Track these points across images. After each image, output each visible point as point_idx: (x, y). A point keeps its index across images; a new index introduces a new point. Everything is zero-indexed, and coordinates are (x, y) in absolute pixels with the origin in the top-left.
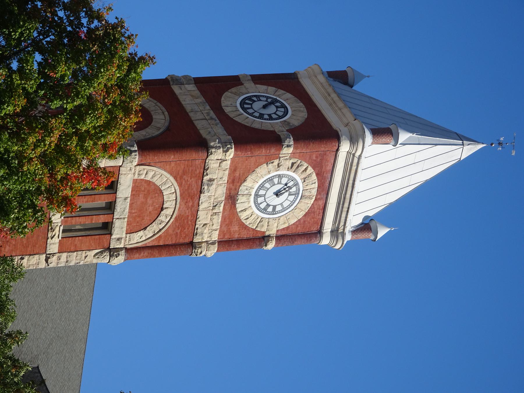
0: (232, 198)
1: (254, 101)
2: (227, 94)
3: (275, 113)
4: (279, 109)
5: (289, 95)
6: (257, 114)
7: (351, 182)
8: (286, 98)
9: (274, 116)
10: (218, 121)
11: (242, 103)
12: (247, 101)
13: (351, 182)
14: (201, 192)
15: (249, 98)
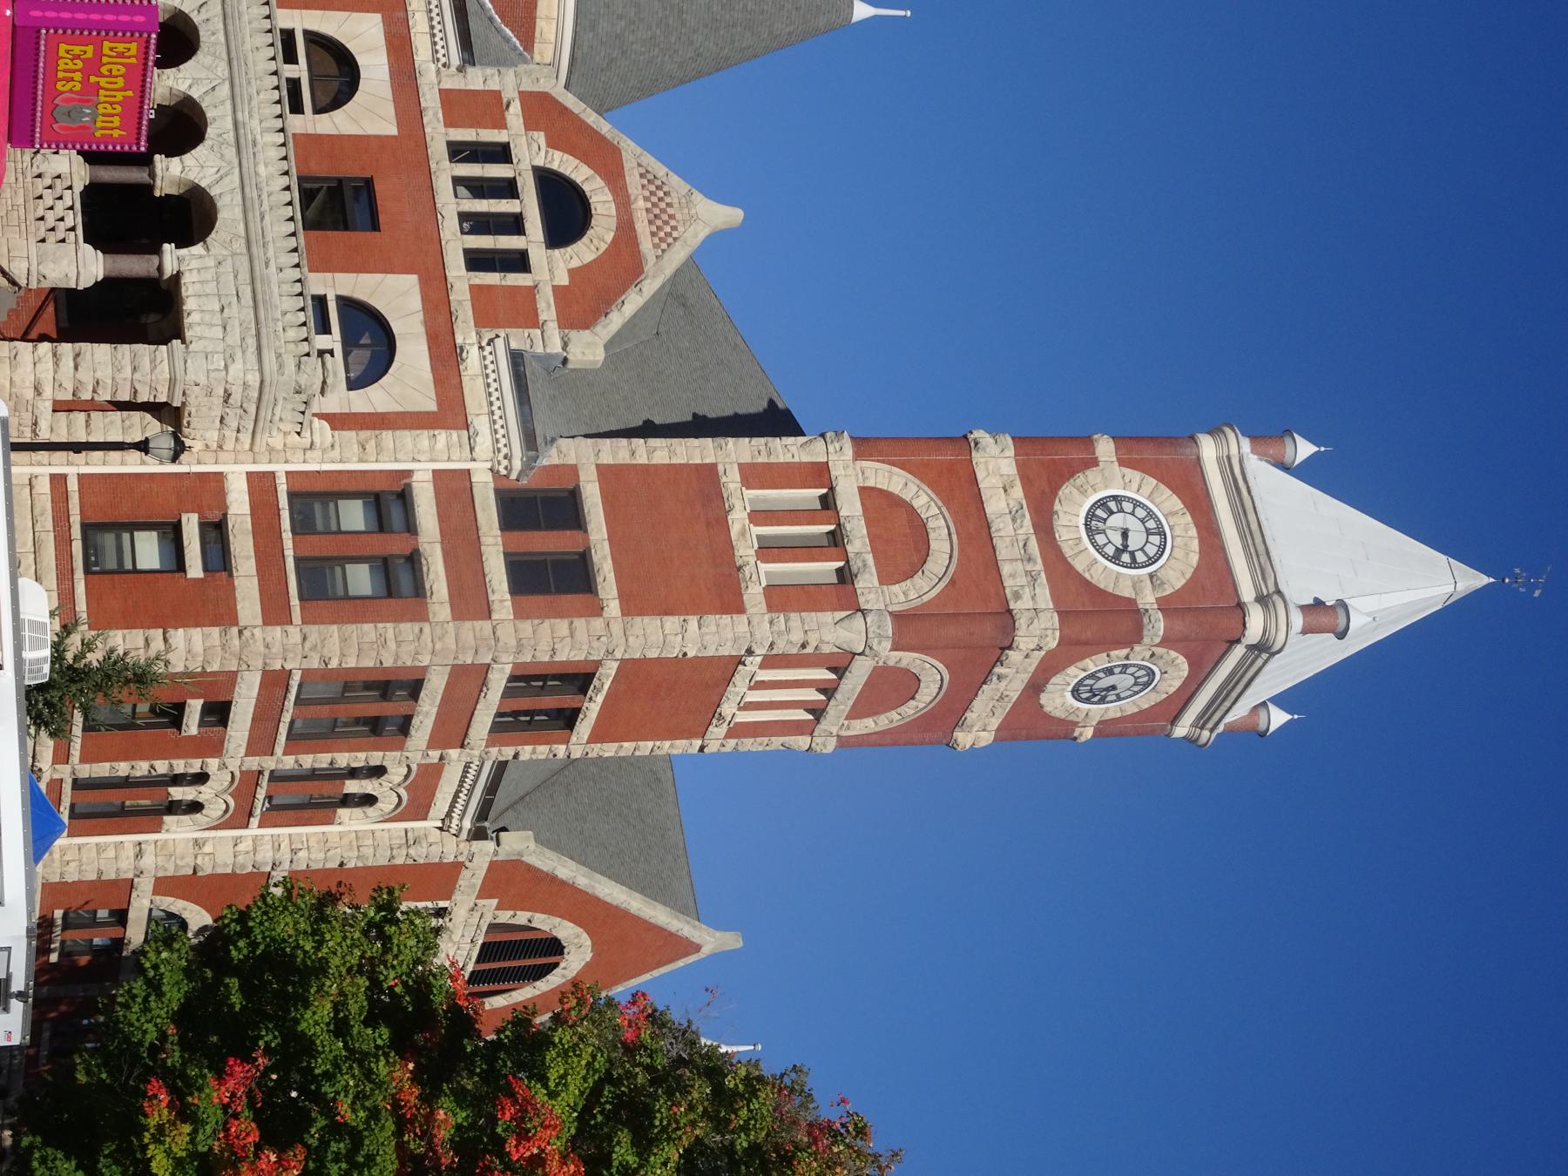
0: (1036, 686)
1: (1112, 513)
2: (1066, 490)
3: (1142, 549)
4: (1151, 538)
5: (1175, 503)
6: (1110, 550)
7: (1245, 680)
8: (1166, 504)
9: (1140, 557)
10: (1039, 566)
11: (1091, 516)
12: (1099, 512)
13: (1245, 680)
14: (984, 682)
15: (1102, 503)
